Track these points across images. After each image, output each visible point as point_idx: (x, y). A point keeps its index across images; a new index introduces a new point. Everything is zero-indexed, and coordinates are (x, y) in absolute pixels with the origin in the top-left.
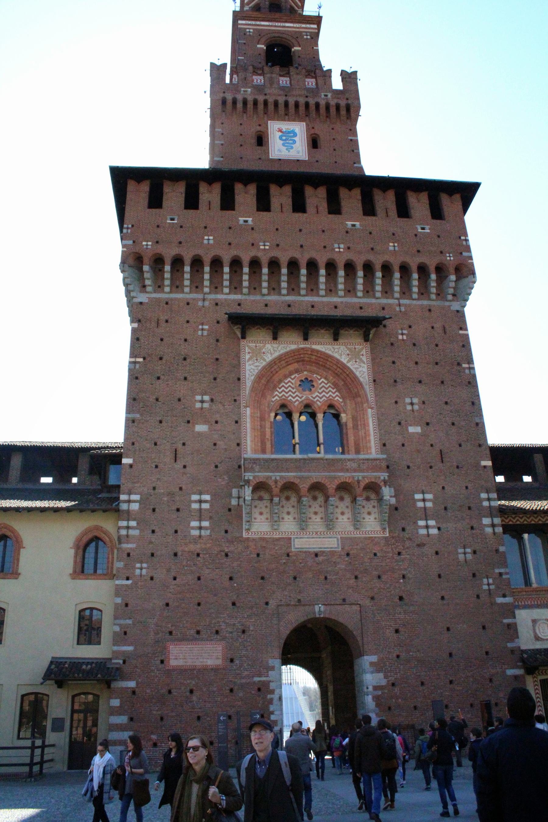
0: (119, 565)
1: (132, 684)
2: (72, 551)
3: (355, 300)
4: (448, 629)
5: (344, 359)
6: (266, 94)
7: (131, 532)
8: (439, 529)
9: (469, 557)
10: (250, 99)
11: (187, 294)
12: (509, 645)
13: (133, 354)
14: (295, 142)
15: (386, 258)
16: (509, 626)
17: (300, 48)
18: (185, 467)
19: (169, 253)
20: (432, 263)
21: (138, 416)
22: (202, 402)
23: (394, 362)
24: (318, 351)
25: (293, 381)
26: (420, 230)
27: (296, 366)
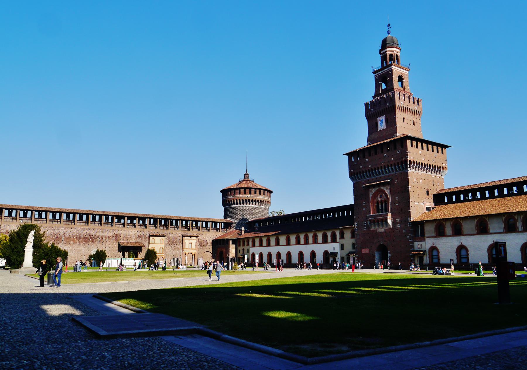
0: (355, 236)
1: (358, 256)
3: (388, 174)
5: (385, 190)
6: (376, 110)
7: (356, 230)
8: (400, 226)
10: (373, 113)
11: (360, 180)
12: (411, 249)
13: (354, 196)
16: (411, 246)
18: (362, 217)
20: (399, 161)
22: (364, 204)
23: (394, 189)
24: (381, 189)
25: (379, 196)
26: (398, 152)
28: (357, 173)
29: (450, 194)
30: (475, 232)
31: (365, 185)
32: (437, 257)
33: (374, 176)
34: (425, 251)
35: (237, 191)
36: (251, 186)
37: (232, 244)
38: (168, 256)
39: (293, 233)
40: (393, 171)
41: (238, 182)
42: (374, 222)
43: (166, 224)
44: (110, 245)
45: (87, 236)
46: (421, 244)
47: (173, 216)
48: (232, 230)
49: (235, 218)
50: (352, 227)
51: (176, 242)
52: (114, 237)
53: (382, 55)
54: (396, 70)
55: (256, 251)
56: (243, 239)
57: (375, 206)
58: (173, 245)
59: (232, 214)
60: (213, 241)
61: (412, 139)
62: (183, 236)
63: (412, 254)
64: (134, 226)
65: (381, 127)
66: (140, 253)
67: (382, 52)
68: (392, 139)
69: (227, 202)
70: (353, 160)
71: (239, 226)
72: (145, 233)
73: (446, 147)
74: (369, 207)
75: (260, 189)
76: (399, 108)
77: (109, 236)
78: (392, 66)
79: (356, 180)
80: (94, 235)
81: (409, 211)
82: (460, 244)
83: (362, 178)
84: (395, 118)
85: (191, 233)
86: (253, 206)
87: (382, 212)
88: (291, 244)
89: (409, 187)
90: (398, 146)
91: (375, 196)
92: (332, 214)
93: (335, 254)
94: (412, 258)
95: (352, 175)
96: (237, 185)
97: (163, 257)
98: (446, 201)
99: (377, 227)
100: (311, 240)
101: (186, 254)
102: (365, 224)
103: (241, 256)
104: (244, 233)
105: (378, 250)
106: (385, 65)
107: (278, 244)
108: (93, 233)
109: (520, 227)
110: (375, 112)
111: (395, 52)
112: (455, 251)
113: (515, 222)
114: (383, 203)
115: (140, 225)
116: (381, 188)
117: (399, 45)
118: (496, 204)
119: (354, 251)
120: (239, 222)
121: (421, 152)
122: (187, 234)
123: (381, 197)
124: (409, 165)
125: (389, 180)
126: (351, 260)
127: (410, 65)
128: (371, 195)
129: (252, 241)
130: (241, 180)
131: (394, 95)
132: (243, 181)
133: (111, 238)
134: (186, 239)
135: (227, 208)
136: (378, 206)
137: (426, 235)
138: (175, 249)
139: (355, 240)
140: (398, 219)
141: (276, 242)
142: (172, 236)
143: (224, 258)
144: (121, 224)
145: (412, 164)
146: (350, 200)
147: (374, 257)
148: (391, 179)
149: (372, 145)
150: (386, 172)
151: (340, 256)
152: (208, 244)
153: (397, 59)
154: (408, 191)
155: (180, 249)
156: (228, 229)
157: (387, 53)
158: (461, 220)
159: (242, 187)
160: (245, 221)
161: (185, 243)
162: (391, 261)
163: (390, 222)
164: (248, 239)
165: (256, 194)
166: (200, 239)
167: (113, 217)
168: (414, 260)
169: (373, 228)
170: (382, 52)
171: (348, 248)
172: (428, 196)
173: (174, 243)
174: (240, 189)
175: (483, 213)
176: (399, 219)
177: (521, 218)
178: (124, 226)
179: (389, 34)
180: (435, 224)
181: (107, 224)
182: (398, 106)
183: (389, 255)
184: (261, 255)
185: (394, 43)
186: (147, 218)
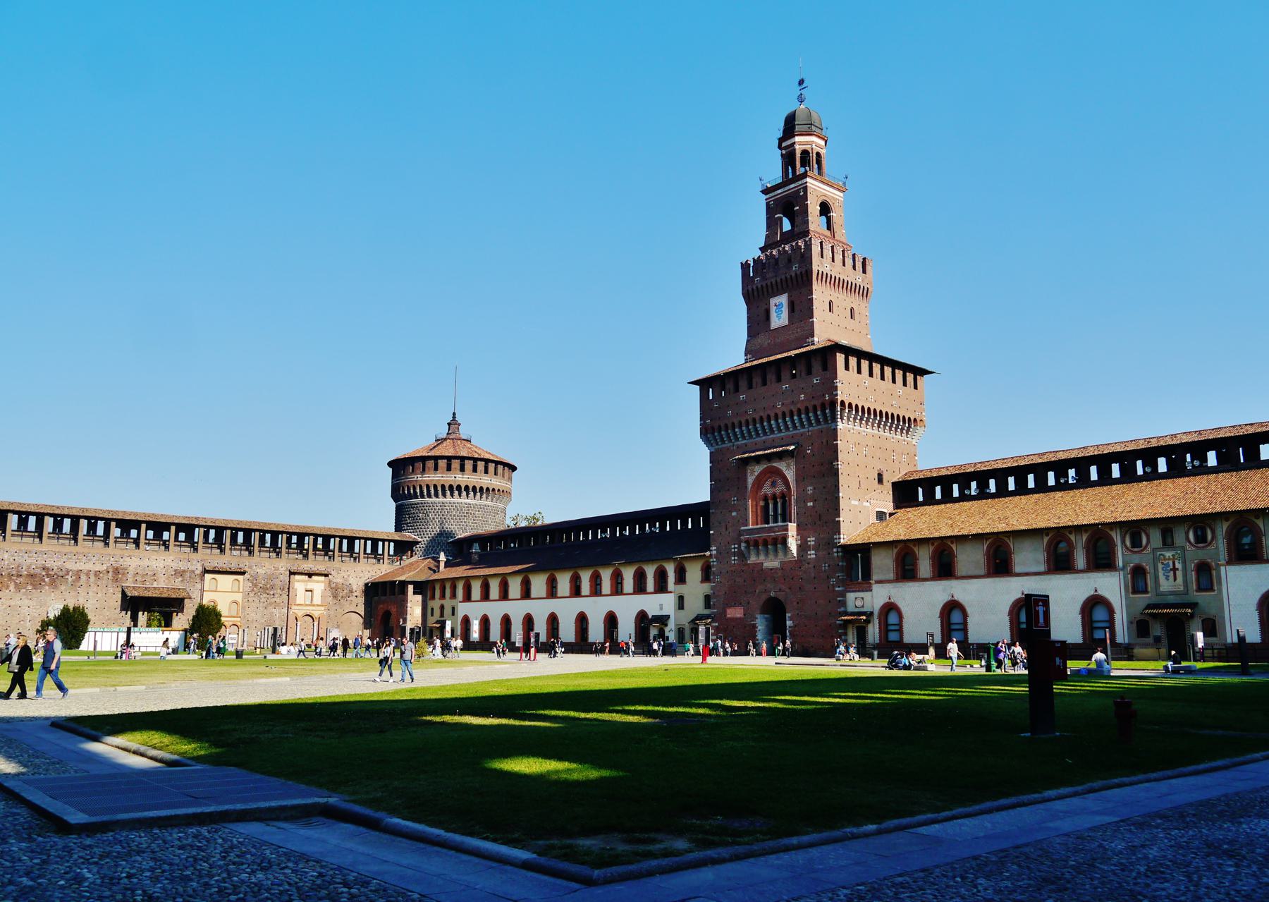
0: (712, 577)
1: (717, 624)
2: (700, 572)
4: (816, 602)
7: (715, 563)
9: (827, 568)
10: (759, 286)
11: (728, 444)
13: (711, 481)
14: (782, 311)
15: (799, 406)
16: (840, 601)
17: (798, 208)
19: (716, 425)
21: (714, 511)
22: (734, 501)
25: (768, 483)
27: (769, 475)
28: (720, 427)
29: (929, 483)
30: (982, 572)
31: (737, 457)
32: (897, 628)
33: (758, 435)
34: (872, 613)
35: (431, 464)
36: (464, 454)
37: (415, 593)
38: (252, 621)
39: (563, 568)
40: (803, 426)
41: (432, 442)
42: (756, 544)
43: (247, 543)
44: (100, 595)
45: (39, 571)
46: (863, 598)
47: (266, 523)
48: (415, 558)
49: (423, 531)
50: (705, 555)
51: (272, 588)
52: (110, 574)
53: (784, 152)
54: (816, 190)
55: (474, 610)
56: (443, 581)
57: (759, 508)
58: (265, 595)
59: (415, 519)
60: (366, 585)
61: (848, 351)
62: (292, 573)
63: (843, 620)
64: (163, 545)
65: (777, 321)
66: (177, 615)
67: (784, 145)
68: (803, 350)
69: (404, 490)
70: (711, 398)
71: (432, 550)
72: (192, 565)
73: (924, 372)
74: (746, 509)
75: (487, 461)
76: (820, 277)
77: (96, 572)
78: (806, 177)
79: (717, 444)
80: (55, 568)
81: (837, 519)
82: (950, 598)
83: (730, 440)
84: (811, 301)
85: (311, 566)
86: (467, 501)
87: (775, 521)
88: (559, 595)
89: (839, 463)
90: (817, 366)
91: (759, 483)
92: (658, 523)
93: (663, 620)
94: (840, 631)
95: (708, 432)
96: (431, 450)
97: (238, 624)
98: (921, 499)
99: (762, 557)
100: (606, 586)
101: (296, 618)
102: (735, 548)
103: (437, 622)
104: (446, 567)
105: (763, 612)
106: (790, 176)
107: (526, 594)
108: (54, 563)
109: (1080, 560)
110: (764, 285)
111: (814, 145)
112: (938, 615)
113: (1071, 547)
114: (778, 500)
115: (179, 544)
116: (775, 465)
117: (824, 129)
118: (1031, 507)
119: (707, 612)
120: (433, 540)
121: (867, 382)
122: (300, 570)
123: (773, 485)
124: (839, 413)
125: (793, 447)
126: (700, 635)
127: (847, 178)
128: (750, 480)
129: (464, 588)
130: (440, 437)
131: (809, 246)
132: (446, 439)
133: (101, 575)
134: (299, 581)
135: (402, 505)
136: (766, 508)
137: (875, 577)
138: (271, 604)
139: (712, 588)
140: (811, 539)
141: (522, 590)
142: (261, 571)
143: (393, 627)
144: (129, 540)
145: (847, 411)
146: (701, 493)
147: (754, 626)
148: (798, 443)
149: (755, 363)
150: (787, 428)
151: (676, 625)
152: (355, 594)
153: (819, 162)
154: (835, 473)
155: (282, 604)
156: (404, 557)
157: (797, 147)
158: (952, 543)
159: (443, 454)
160: (447, 537)
161: (296, 589)
162: (792, 635)
163: (793, 544)
164: (454, 581)
165: (476, 472)
166: (334, 580)
167: (107, 522)
168: (846, 634)
169: (753, 559)
170: (784, 145)
171: (696, 605)
172: (880, 486)
173: (267, 589)
174: (436, 458)
175: (1002, 527)
176: (814, 539)
177: (1084, 540)
178: (138, 546)
179: (801, 102)
180: (895, 551)
181: (93, 540)
182: (818, 273)
183: (789, 623)
184: (485, 622)
185: (811, 124)
186: (199, 526)
